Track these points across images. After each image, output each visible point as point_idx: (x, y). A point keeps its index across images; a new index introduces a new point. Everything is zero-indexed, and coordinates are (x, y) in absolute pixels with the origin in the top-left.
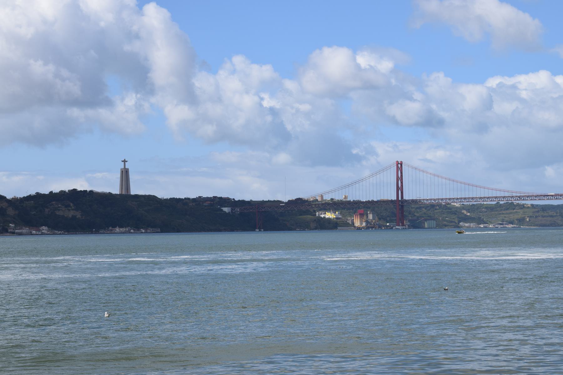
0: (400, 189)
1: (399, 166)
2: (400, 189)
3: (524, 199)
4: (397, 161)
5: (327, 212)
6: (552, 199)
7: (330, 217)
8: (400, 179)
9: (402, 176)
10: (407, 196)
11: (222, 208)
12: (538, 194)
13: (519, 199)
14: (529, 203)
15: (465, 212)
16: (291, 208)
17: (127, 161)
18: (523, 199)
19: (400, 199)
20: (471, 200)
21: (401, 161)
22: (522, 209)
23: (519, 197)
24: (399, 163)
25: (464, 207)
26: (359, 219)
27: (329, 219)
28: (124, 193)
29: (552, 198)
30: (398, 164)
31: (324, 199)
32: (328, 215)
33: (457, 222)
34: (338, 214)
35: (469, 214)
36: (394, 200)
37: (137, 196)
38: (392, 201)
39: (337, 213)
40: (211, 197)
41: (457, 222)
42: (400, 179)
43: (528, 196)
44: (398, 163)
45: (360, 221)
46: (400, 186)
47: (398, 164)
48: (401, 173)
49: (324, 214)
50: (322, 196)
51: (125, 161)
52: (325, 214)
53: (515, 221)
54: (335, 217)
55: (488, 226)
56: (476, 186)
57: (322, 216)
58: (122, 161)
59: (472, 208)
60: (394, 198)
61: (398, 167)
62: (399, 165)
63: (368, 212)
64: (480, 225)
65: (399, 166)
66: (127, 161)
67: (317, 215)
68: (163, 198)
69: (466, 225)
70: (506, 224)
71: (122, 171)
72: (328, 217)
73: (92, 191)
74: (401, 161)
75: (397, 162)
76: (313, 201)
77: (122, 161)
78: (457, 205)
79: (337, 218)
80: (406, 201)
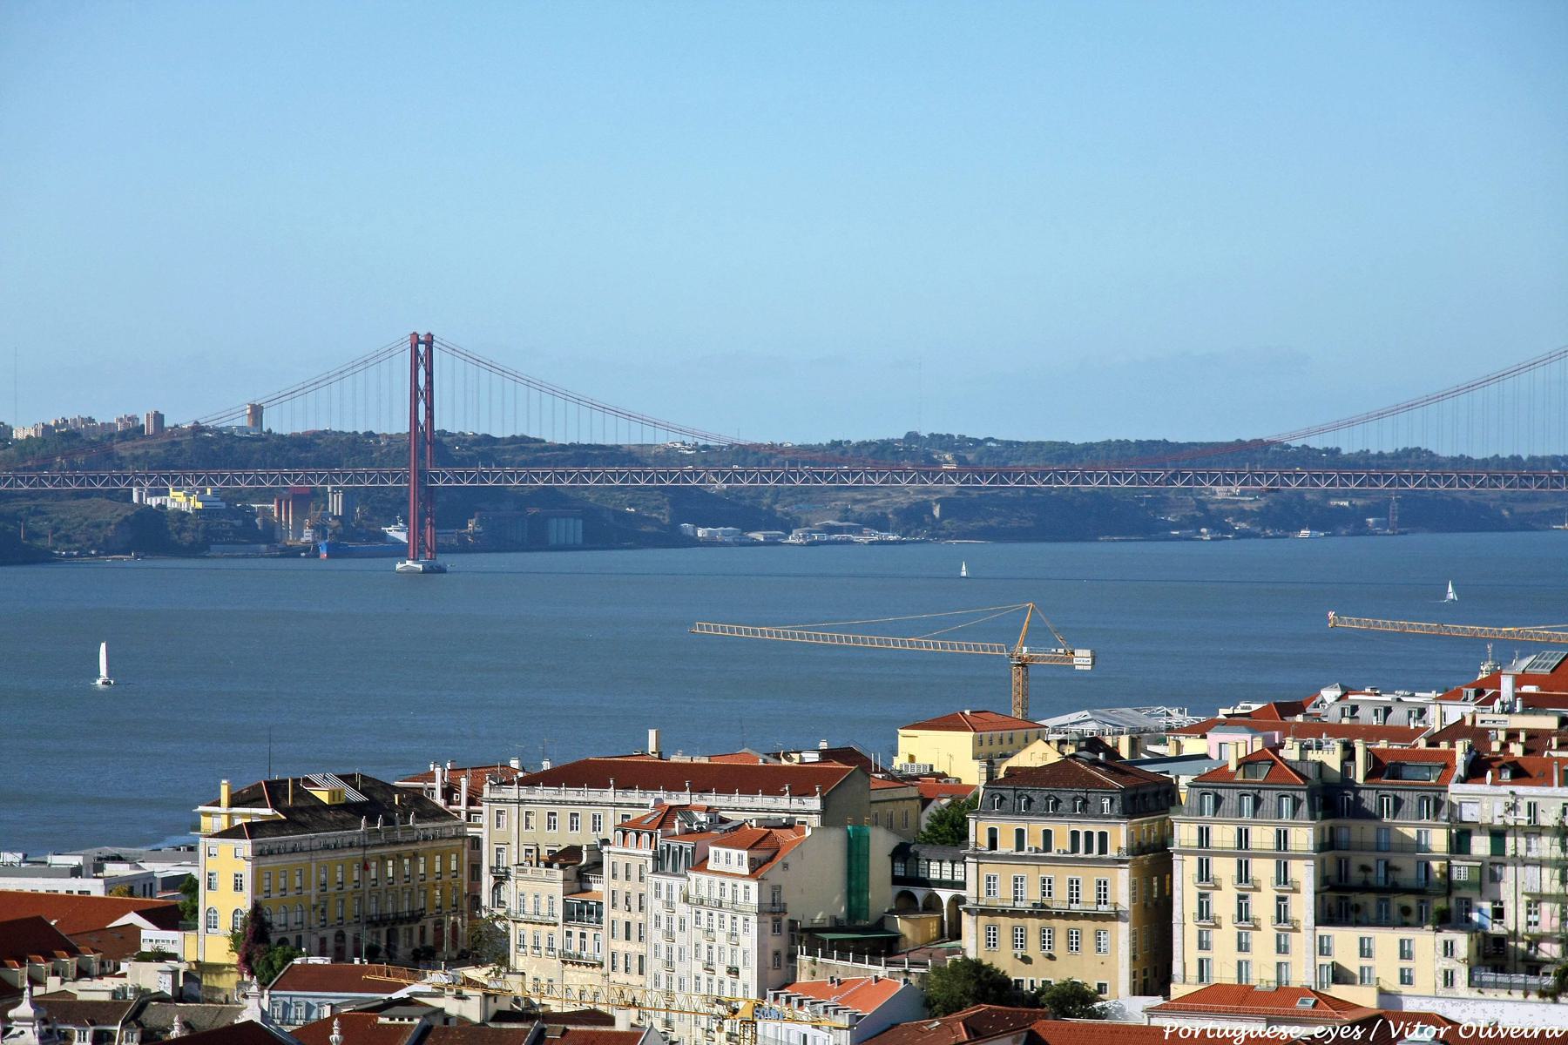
1: (422, 350)
4: (415, 333)
7: (184, 508)
9: (430, 382)
21: (429, 334)
24: (422, 338)
30: (419, 342)
31: (168, 423)
44: (416, 340)
46: (422, 418)
48: (429, 374)
50: (159, 418)
52: (167, 493)
54: (199, 505)
57: (154, 502)
61: (415, 352)
62: (422, 348)
65: (422, 350)
67: (135, 499)
69: (699, 534)
72: (174, 505)
74: (429, 334)
75: (416, 340)
76: (124, 436)
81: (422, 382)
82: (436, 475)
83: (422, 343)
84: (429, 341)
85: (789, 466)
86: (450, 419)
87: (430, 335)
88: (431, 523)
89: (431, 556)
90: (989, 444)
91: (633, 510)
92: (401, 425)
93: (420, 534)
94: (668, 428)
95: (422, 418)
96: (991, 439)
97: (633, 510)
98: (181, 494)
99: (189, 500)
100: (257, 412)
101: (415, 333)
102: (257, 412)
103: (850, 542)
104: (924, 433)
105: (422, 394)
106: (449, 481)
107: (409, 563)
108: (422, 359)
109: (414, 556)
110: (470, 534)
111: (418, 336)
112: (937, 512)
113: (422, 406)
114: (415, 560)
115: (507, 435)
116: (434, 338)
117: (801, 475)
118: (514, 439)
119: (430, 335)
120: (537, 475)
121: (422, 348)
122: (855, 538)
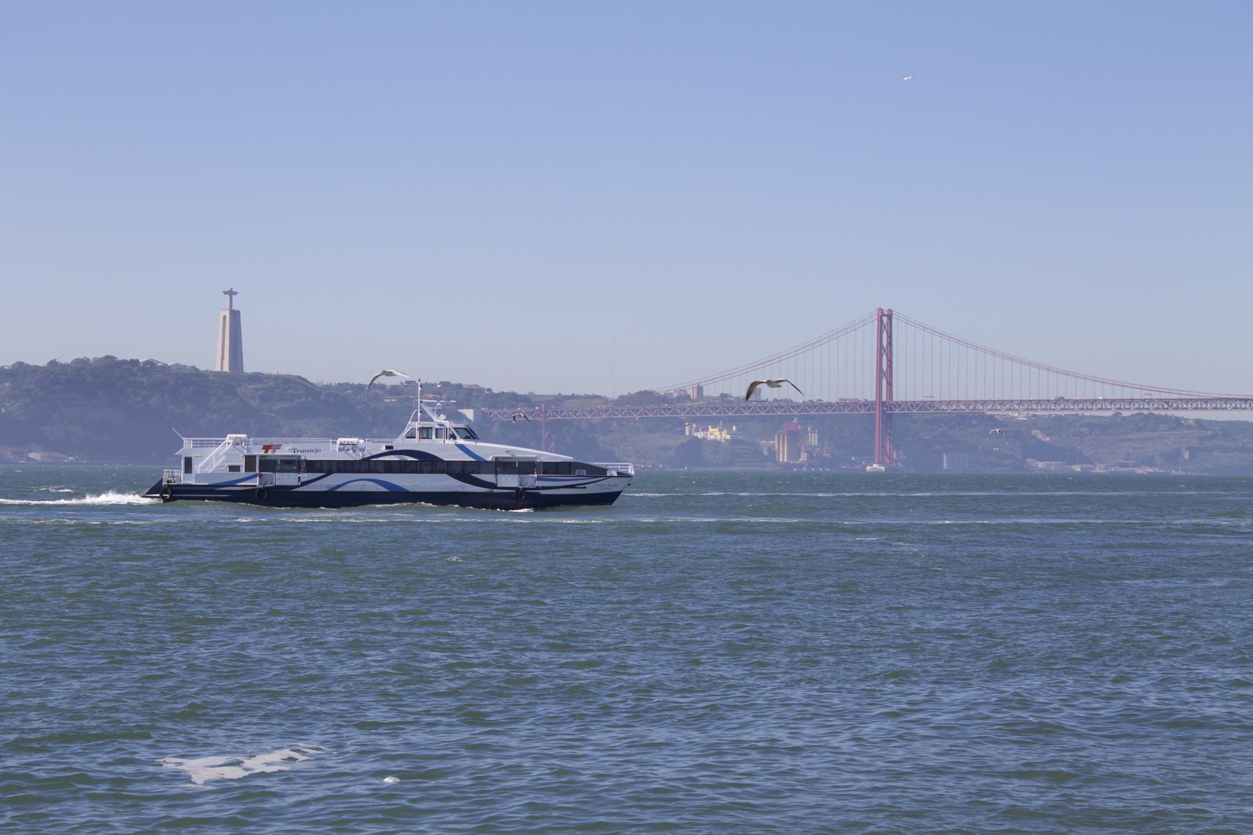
0: (885, 375)
1: (885, 321)
2: (885, 375)
3: (1178, 406)
4: (880, 309)
5: (710, 427)
6: (1245, 408)
7: (719, 437)
8: (885, 350)
10: (904, 392)
11: (460, 411)
12: (1211, 395)
13: (1166, 406)
14: (1190, 415)
15: (1037, 433)
16: (626, 414)
17: (235, 293)
18: (1175, 405)
19: (884, 399)
20: (1053, 407)
21: (890, 310)
22: (1174, 429)
23: (1167, 401)
24: (885, 313)
25: (1035, 422)
26: (786, 445)
27: (716, 443)
28: (226, 369)
29: (1243, 406)
30: (883, 315)
31: (706, 393)
32: (712, 434)
33: (1019, 457)
34: (737, 429)
35: (1048, 439)
36: (871, 402)
37: (257, 378)
38: (867, 405)
39: (734, 428)
40: (435, 385)
41: (1019, 457)
42: (885, 350)
43: (1188, 401)
44: (881, 314)
45: (788, 446)
47: (883, 315)
48: (890, 337)
49: (703, 430)
50: (700, 389)
51: (231, 293)
52: (707, 429)
53: (1158, 458)
54: (728, 437)
55: (1091, 468)
56: (1066, 374)
57: (700, 435)
58: (225, 293)
59: (1055, 425)
60: (871, 397)
61: (881, 322)
62: (885, 319)
63: (809, 429)
64: (1073, 467)
65: (885, 321)
66: (235, 293)
67: (687, 433)
68: (322, 383)
69: (1040, 466)
70: (1134, 465)
71: (225, 317)
72: (712, 437)
73: (152, 362)
74: (890, 310)
75: (881, 310)
76: (679, 399)
77: (225, 293)
78: (1020, 416)
79: (733, 441)
80: (898, 405)
83: (885, 316)
88: (890, 439)
91: (997, 449)
93: (883, 446)
97: (997, 449)
98: (717, 430)
99: (721, 434)
101: (880, 309)
107: (875, 465)
108: (885, 327)
109: (879, 460)
111: (882, 310)
114: (879, 463)
121: (885, 319)
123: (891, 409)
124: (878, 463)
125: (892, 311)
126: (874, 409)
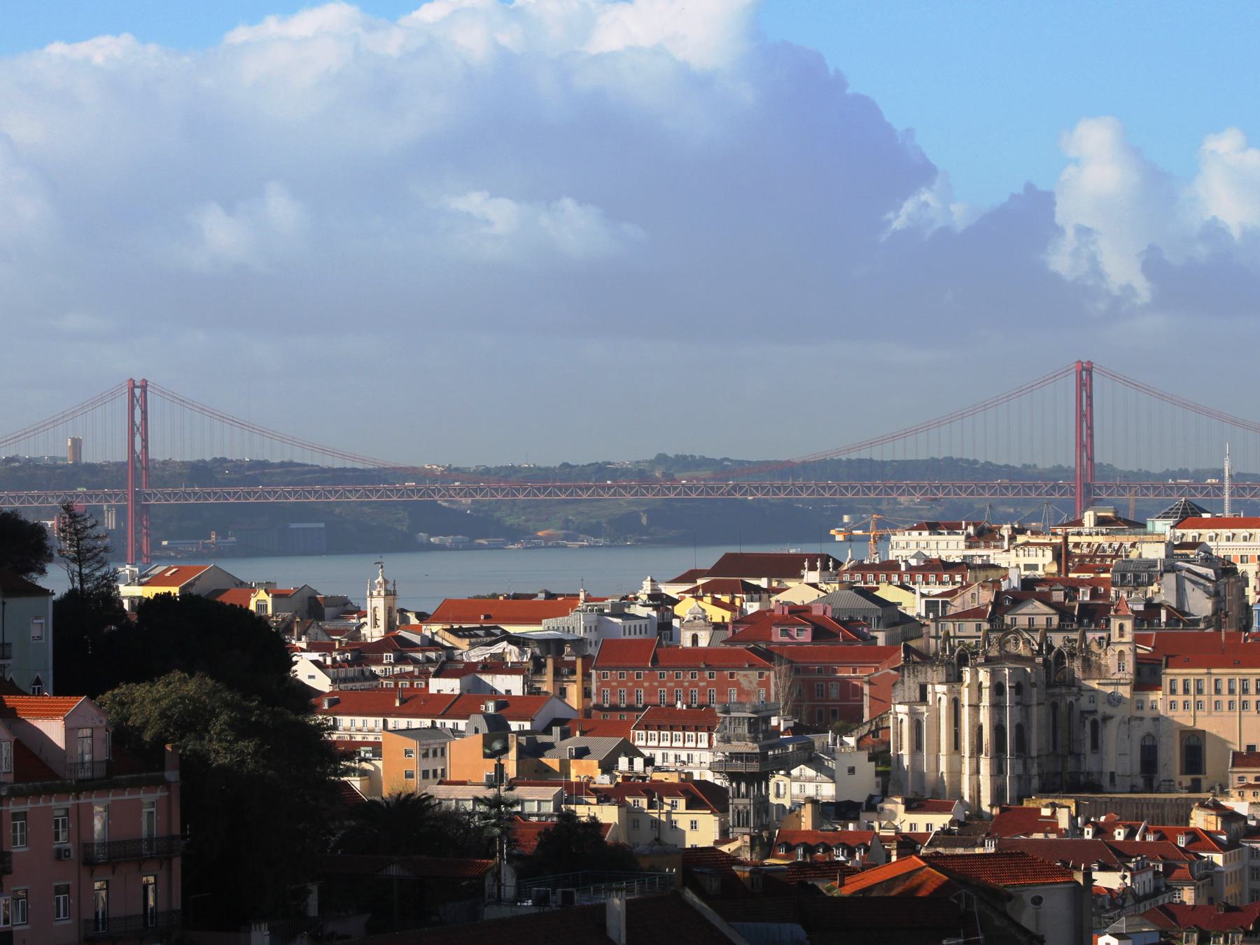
1: (138, 393)
4: (131, 379)
21: (144, 380)
30: (135, 386)
44: (133, 385)
46: (138, 447)
47: (135, 386)
61: (132, 395)
62: (138, 392)
74: (144, 380)
75: (132, 381)
81: (138, 419)
82: (149, 495)
83: (138, 387)
84: (144, 387)
85: (185, 487)
86: (158, 453)
87: (145, 381)
89: (147, 560)
90: (726, 463)
92: (121, 455)
94: (343, 456)
95: (138, 447)
96: (727, 459)
100: (77, 445)
102: (77, 445)
103: (565, 546)
104: (671, 454)
105: (138, 428)
106: (159, 500)
110: (213, 544)
111: (134, 381)
112: (644, 520)
113: (138, 439)
115: (277, 460)
116: (148, 383)
117: (439, 491)
118: (282, 464)
119: (145, 381)
120: (229, 493)
121: (138, 392)
122: (570, 544)
123: (146, 500)
124: (132, 564)
125: (146, 382)
126: (126, 500)
